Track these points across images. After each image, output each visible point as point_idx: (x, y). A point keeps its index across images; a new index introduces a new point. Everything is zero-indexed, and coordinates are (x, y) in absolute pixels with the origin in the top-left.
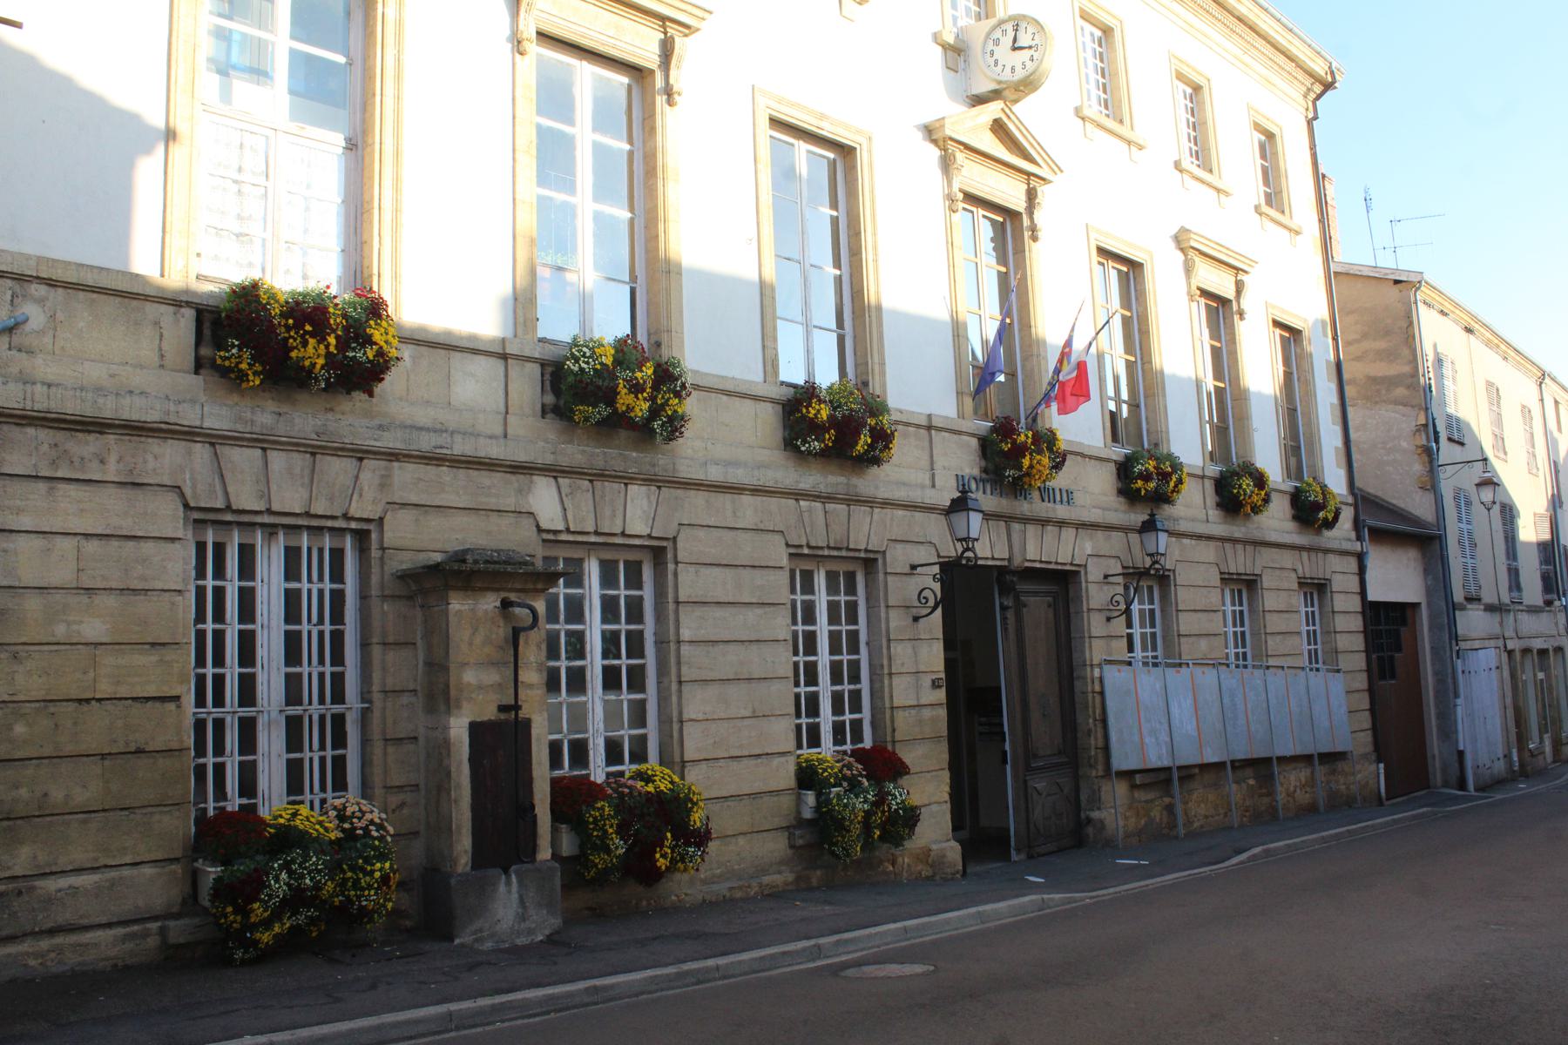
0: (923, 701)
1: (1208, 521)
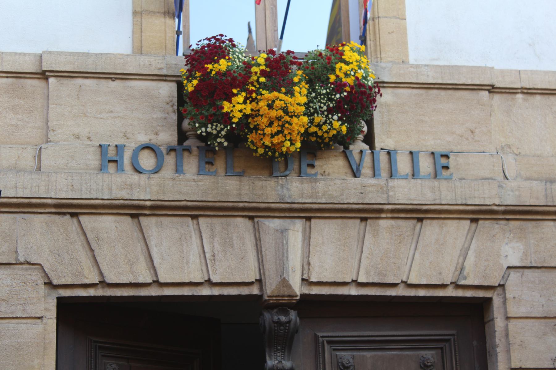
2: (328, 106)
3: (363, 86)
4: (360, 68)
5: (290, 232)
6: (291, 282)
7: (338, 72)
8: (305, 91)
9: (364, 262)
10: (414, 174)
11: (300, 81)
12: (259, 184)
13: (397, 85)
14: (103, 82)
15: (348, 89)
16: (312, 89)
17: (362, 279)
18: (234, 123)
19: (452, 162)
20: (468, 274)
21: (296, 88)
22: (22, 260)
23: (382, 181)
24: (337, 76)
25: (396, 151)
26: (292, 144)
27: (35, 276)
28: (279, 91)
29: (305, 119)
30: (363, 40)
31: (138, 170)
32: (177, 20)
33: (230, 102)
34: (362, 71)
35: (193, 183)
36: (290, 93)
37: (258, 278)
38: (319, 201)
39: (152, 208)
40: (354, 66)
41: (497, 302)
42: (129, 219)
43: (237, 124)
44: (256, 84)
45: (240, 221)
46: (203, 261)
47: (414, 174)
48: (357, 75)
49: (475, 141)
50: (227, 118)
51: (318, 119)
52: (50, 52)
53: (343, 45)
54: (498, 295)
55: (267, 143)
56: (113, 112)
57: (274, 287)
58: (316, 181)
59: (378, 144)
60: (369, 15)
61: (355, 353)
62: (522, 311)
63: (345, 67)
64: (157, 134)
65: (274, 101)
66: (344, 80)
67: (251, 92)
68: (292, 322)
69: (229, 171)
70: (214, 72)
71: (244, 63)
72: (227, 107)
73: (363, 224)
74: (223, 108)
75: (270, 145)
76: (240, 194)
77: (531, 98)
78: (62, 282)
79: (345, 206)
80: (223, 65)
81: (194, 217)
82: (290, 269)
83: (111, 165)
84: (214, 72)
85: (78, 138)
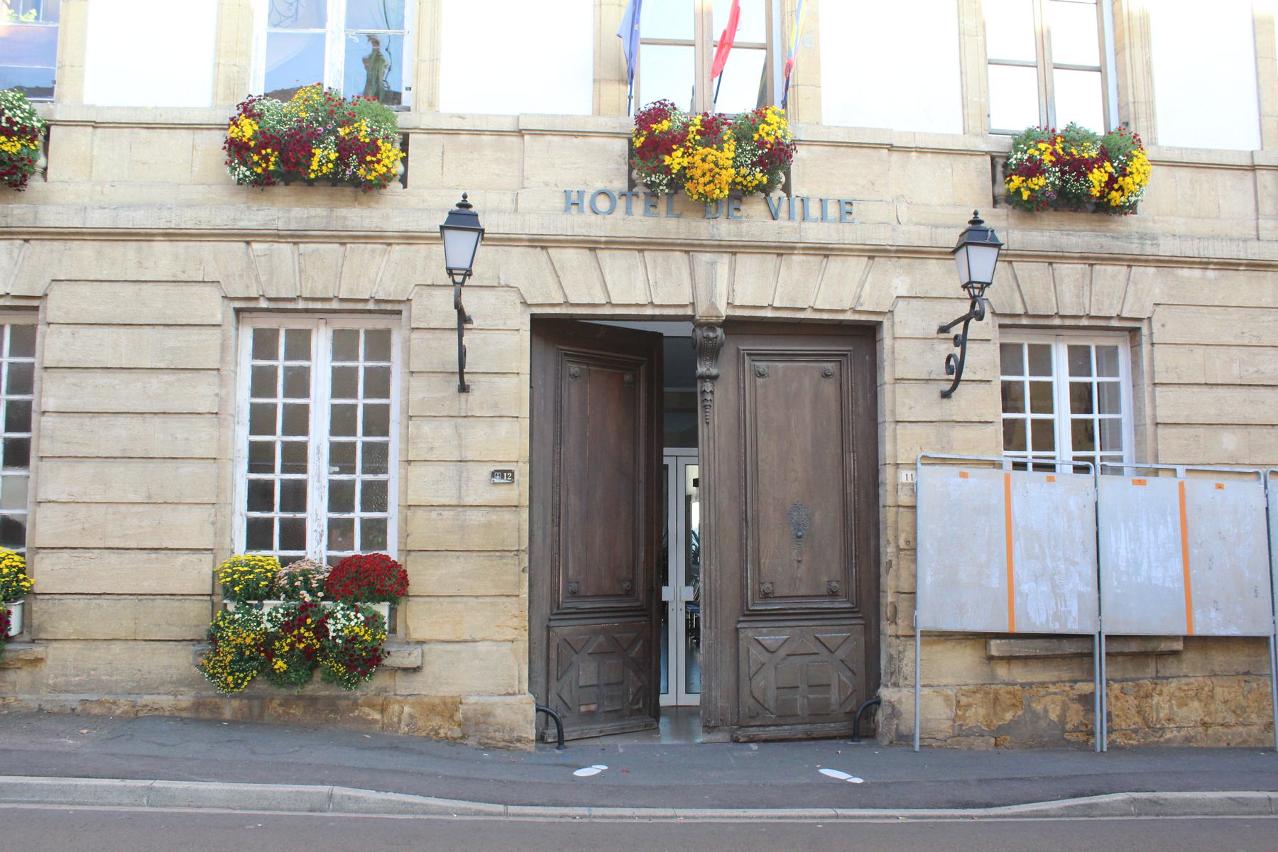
0: (470, 500)
1: (1258, 239)
3: (782, 144)
4: (779, 129)
5: (719, 264)
7: (761, 132)
8: (733, 148)
9: (779, 290)
11: (729, 139)
12: (693, 224)
13: (811, 143)
14: (568, 138)
15: (769, 146)
16: (739, 145)
17: (776, 304)
19: (855, 209)
21: (726, 145)
22: (503, 284)
23: (795, 224)
24: (760, 135)
25: (808, 198)
26: (721, 192)
27: (513, 297)
28: (711, 148)
29: (732, 171)
30: (784, 105)
31: (596, 212)
32: (629, 86)
33: (671, 156)
34: (781, 131)
36: (721, 149)
38: (743, 239)
39: (606, 243)
41: (886, 325)
42: (587, 252)
43: (676, 174)
44: (692, 141)
46: (647, 287)
50: (667, 170)
51: (744, 171)
53: (766, 109)
55: (701, 190)
57: (704, 308)
58: (741, 222)
59: (794, 193)
60: (790, 84)
61: (770, 364)
62: (906, 333)
64: (611, 182)
65: (707, 156)
66: (766, 139)
67: (688, 148)
69: (670, 212)
70: (657, 131)
71: (683, 123)
72: (668, 160)
73: (779, 258)
74: (664, 161)
77: (923, 156)
78: (535, 302)
80: (665, 125)
81: (641, 251)
83: (573, 207)
84: (657, 131)
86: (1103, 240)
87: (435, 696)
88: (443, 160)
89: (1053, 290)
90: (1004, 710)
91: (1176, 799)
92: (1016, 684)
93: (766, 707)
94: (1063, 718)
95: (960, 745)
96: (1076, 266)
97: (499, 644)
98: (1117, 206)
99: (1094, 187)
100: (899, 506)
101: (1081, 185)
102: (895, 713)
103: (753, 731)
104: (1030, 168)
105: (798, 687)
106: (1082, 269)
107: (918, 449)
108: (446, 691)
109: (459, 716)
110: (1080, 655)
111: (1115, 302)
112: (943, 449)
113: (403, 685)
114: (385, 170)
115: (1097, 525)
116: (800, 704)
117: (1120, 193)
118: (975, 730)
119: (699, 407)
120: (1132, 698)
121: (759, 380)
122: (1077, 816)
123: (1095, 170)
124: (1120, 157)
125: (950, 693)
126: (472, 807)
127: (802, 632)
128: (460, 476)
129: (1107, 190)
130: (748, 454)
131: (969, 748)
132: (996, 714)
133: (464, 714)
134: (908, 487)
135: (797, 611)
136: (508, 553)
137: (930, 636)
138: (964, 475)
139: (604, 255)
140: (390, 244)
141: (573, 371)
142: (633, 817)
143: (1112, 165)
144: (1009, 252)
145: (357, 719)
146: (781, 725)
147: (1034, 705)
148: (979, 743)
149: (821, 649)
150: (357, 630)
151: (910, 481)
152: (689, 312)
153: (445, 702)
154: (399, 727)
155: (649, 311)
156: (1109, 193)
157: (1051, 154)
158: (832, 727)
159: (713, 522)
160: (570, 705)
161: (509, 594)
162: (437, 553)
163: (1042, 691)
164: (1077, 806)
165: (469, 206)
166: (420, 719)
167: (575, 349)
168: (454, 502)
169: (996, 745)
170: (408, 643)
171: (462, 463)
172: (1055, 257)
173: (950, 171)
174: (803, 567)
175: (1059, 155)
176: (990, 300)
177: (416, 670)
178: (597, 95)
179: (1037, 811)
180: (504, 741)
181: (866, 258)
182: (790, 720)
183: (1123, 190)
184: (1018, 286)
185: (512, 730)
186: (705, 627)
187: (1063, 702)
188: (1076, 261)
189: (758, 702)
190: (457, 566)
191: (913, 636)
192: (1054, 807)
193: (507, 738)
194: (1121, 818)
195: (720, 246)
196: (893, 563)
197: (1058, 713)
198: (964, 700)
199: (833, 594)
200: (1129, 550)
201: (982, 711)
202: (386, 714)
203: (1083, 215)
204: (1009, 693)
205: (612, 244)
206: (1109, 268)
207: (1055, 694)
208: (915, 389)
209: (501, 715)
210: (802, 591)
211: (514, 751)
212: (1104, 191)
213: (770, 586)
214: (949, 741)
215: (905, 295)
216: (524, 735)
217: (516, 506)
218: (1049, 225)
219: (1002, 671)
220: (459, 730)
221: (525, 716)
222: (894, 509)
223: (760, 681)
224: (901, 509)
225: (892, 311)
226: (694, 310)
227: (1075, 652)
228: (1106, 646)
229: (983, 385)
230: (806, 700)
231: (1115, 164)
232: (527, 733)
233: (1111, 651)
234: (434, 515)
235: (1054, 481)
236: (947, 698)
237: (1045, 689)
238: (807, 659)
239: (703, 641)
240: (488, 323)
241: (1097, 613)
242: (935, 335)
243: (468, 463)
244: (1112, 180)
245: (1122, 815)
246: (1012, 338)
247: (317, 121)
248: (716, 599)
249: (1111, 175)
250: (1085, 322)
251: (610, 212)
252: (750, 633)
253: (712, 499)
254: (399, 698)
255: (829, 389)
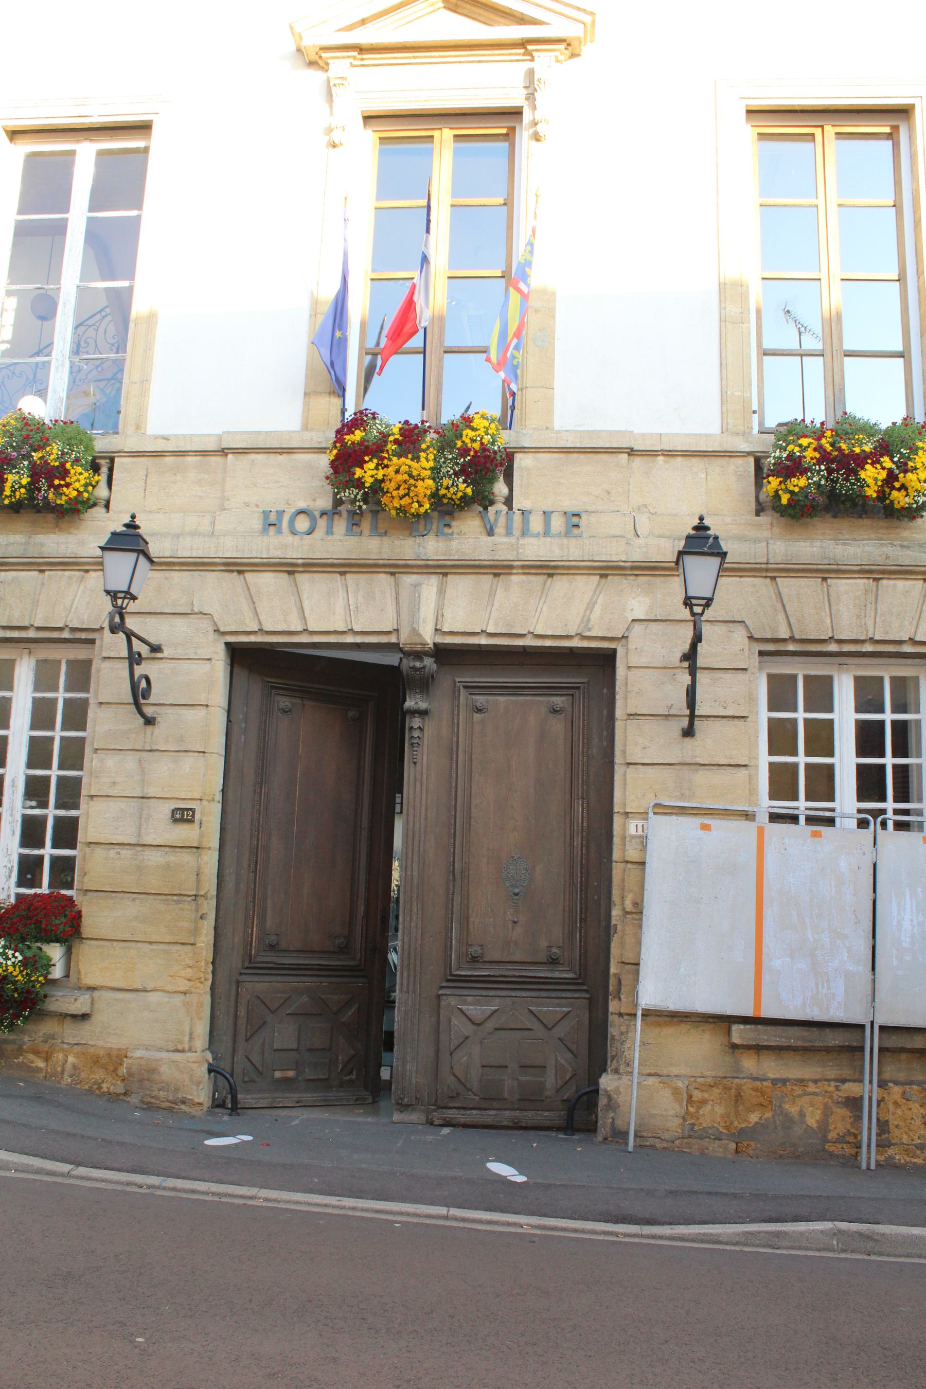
2: (454, 470)
3: (488, 450)
5: (424, 586)
6: (421, 632)
7: (464, 438)
8: (431, 457)
9: (494, 614)
10: (547, 533)
11: (428, 447)
12: (398, 543)
13: (538, 450)
14: (272, 456)
15: (472, 453)
17: (490, 630)
18: (366, 488)
20: (593, 626)
21: (423, 455)
22: (196, 610)
23: (512, 540)
24: (463, 442)
26: (421, 506)
27: (206, 625)
29: (430, 482)
31: (294, 533)
33: (362, 468)
34: (489, 437)
35: (339, 543)
36: (417, 458)
37: (396, 628)
38: (452, 558)
39: (304, 565)
40: (481, 432)
42: (286, 575)
45: (382, 576)
46: (348, 612)
47: (547, 533)
48: (483, 441)
49: (611, 501)
50: (359, 484)
52: (229, 432)
54: (622, 646)
56: (277, 482)
57: (406, 635)
58: (450, 540)
61: (490, 698)
62: (644, 661)
63: (471, 433)
64: (314, 500)
66: (469, 445)
67: (383, 459)
68: (427, 669)
69: (376, 531)
72: (358, 472)
73: (497, 579)
74: (354, 474)
75: (398, 506)
76: (380, 553)
77: (672, 460)
78: (228, 629)
79: (477, 563)
81: (343, 574)
82: (421, 619)
83: (271, 528)
84: (350, 442)
85: (248, 506)
86: (889, 550)
87: (102, 1048)
88: (146, 483)
89: (827, 610)
90: (749, 1110)
91: (897, 1235)
92: (765, 1080)
93: (468, 1086)
94: (824, 1125)
95: (690, 1148)
96: (857, 581)
97: (171, 995)
98: (902, 508)
99: (868, 486)
100: (627, 862)
101: (853, 484)
102: (612, 1105)
103: (451, 1114)
104: (788, 467)
105: (507, 1067)
106: (864, 584)
107: (652, 795)
108: (114, 1042)
109: (123, 1070)
110: (842, 1049)
111: (907, 623)
112: (682, 797)
113: (70, 1033)
114: (75, 493)
115: (874, 891)
116: (509, 1084)
117: (903, 493)
118: (710, 1131)
119: (406, 745)
120: (917, 1105)
121: (477, 717)
122: (758, 1246)
123: (868, 467)
124: (902, 450)
125: (680, 1084)
126: (35, 1163)
127: (514, 1003)
128: (141, 814)
129: (887, 490)
130: (459, 797)
131: (703, 1154)
132: (737, 1114)
133: (128, 1068)
134: (638, 840)
135: (508, 979)
136: (185, 898)
137: (659, 1016)
138: (706, 827)
139: (302, 578)
140: (87, 571)
141: (282, 705)
142: (207, 1193)
143: (892, 460)
144: (770, 566)
145: (20, 1066)
146: (486, 1109)
147: (787, 1106)
148: (715, 1148)
149: (536, 1025)
150: (11, 969)
151: (640, 832)
152: (393, 639)
153: (109, 1054)
154: (62, 1077)
155: (349, 639)
156: (890, 494)
157: (815, 450)
158: (545, 1117)
159: (415, 873)
160: (261, 1069)
161: (183, 942)
162: (113, 895)
163: (798, 1091)
164: (760, 1232)
165: (137, 527)
166: (83, 1071)
167: (286, 682)
168: (133, 841)
169: (737, 1151)
170: (80, 988)
171: (144, 800)
172: (828, 571)
173: (703, 476)
174: (519, 929)
175: (825, 450)
176: (747, 623)
177: (85, 1017)
178: (307, 409)
179: (704, 1234)
180: (168, 1101)
181: (598, 577)
182: (495, 1104)
183: (906, 489)
184: (784, 606)
185: (177, 1090)
186: (401, 991)
187: (826, 1106)
188: (857, 576)
189: (459, 1080)
190: (131, 909)
191: (635, 1015)
192: (729, 1231)
193: (171, 1098)
194: (817, 1254)
195: (427, 566)
196: (619, 928)
197: (818, 1118)
198: (697, 1095)
199: (553, 962)
200: (915, 922)
201: (720, 1110)
202: (50, 1062)
203: (867, 522)
204: (755, 1090)
205: (311, 566)
206: (900, 584)
207: (814, 1094)
208: (649, 726)
209: (167, 1072)
210: (517, 957)
211: (177, 1113)
212: (884, 491)
213: (478, 949)
214: (677, 1142)
215: (643, 618)
216: (189, 1097)
217: (198, 848)
218: (824, 534)
219: (749, 1063)
220: (122, 1085)
221: (192, 1076)
222: (622, 865)
223: (461, 1058)
224: (629, 866)
225: (627, 637)
226: (398, 638)
227: (841, 1044)
228: (880, 1039)
229: (736, 722)
230: (515, 1084)
231: (896, 459)
232: (191, 1094)
233: (888, 1045)
234: (112, 853)
235: (821, 836)
236: (676, 1092)
237: (802, 1088)
238: (518, 1035)
239: (398, 1007)
240: (179, 653)
241: (870, 999)
242: (678, 664)
243: (150, 800)
244: (891, 477)
245: (819, 1250)
246: (783, 668)
247: (12, 447)
248: (415, 960)
249: (890, 472)
250: (868, 648)
251: (310, 532)
252: (453, 1001)
253: (416, 848)
254: (65, 1046)
255: (558, 726)
